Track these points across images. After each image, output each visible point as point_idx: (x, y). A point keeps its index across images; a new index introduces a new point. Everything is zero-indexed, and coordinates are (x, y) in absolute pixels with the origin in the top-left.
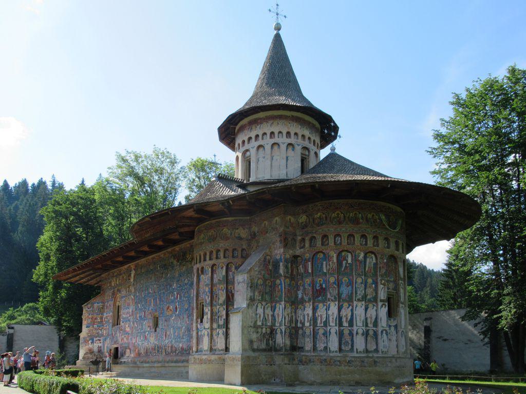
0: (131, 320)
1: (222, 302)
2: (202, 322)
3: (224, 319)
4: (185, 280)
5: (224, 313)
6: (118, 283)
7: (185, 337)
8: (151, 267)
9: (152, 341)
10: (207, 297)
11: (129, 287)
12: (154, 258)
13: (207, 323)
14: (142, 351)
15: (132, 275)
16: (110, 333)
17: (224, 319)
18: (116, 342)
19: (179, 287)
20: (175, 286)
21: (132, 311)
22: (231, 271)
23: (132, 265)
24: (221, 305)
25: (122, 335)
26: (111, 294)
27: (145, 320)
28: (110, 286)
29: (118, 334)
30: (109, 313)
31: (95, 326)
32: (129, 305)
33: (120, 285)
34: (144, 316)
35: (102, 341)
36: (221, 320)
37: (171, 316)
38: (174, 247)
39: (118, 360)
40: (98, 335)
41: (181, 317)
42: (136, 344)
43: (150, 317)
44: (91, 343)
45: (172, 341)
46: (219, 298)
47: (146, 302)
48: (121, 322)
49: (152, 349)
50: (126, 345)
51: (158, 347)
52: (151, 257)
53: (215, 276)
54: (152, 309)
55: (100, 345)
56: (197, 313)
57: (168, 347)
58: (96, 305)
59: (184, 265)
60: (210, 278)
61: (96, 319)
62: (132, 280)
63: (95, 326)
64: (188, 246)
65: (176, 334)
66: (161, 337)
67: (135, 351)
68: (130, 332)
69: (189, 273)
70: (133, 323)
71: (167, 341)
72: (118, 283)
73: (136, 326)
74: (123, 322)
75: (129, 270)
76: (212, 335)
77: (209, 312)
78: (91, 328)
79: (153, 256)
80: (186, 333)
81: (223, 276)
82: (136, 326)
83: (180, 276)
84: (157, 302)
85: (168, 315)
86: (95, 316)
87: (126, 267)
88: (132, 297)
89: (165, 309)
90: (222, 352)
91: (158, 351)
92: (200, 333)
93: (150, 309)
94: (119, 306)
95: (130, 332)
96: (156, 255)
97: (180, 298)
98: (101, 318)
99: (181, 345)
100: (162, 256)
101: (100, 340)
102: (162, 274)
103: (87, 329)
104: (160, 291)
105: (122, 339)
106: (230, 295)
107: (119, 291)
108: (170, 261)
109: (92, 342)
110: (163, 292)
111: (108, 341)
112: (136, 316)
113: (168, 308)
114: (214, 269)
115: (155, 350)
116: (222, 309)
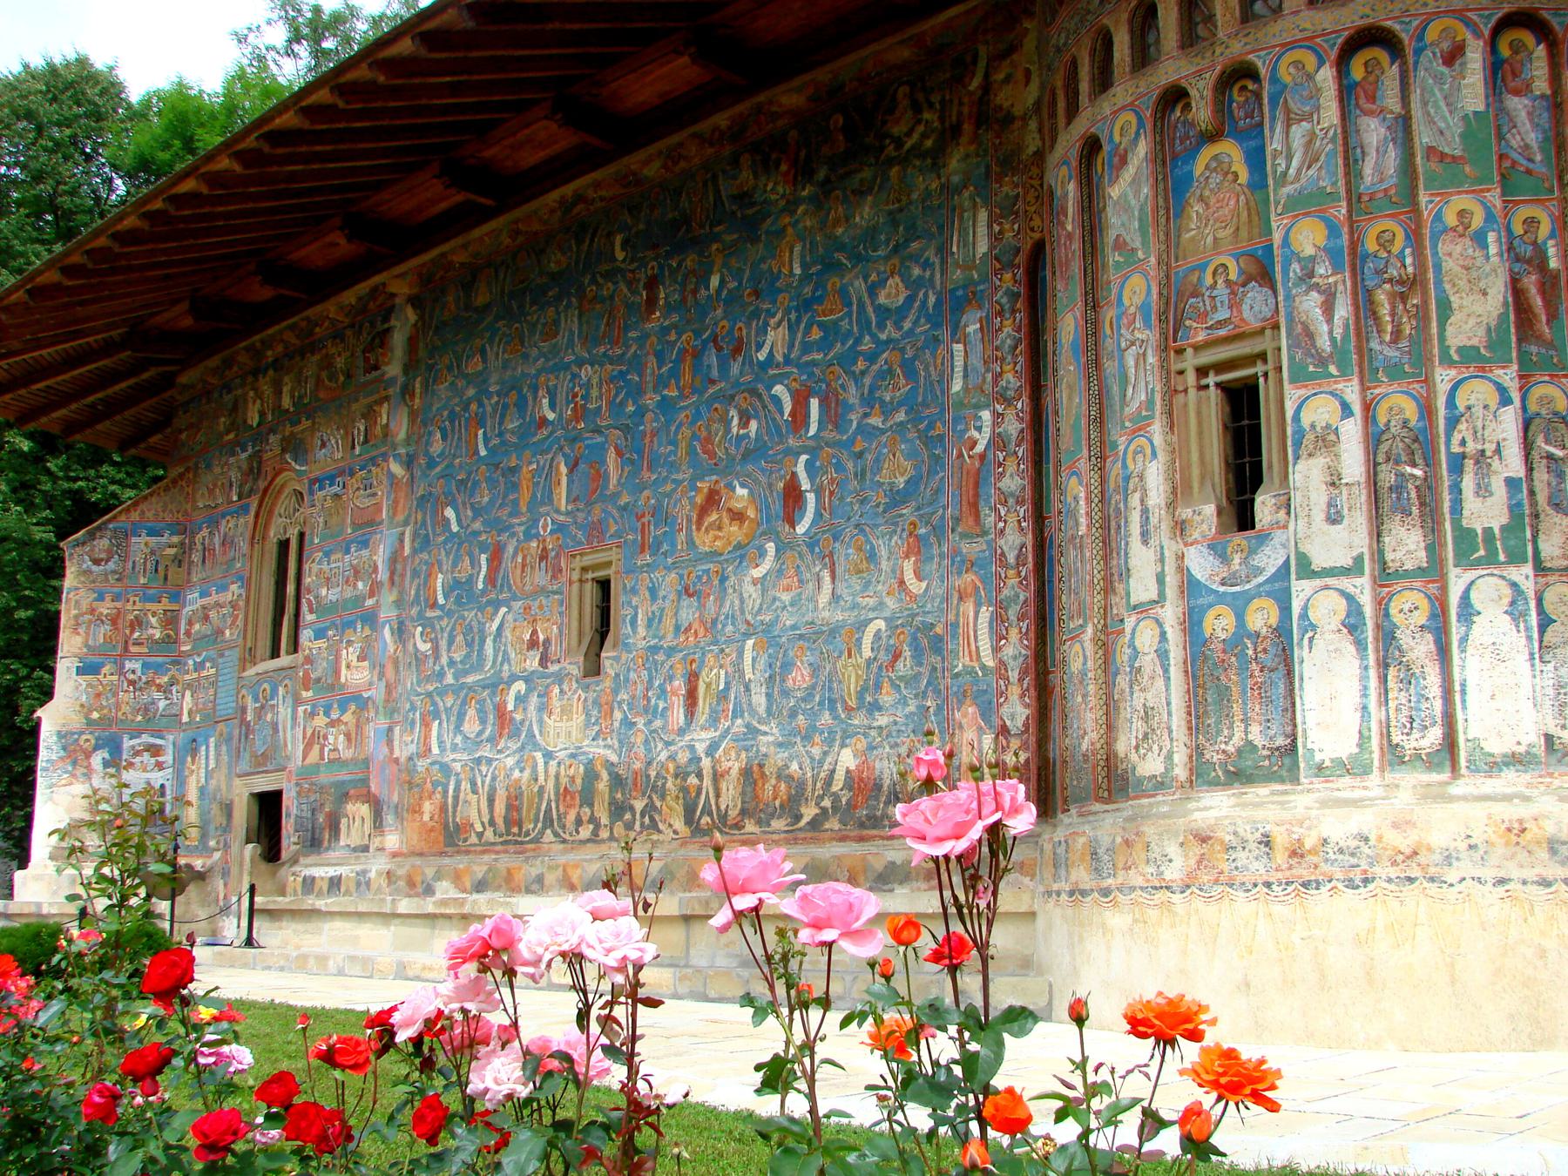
0: (387, 612)
1: (1477, 338)
2: (1243, 518)
3: (1511, 483)
4: (873, 291)
5: (1508, 425)
6: (286, 402)
7: (887, 698)
8: (555, 261)
9: (569, 732)
10: (1311, 304)
11: (370, 414)
12: (579, 198)
13: (1334, 519)
14: (473, 811)
15: (398, 340)
16: (227, 705)
17: (1511, 483)
18: (262, 762)
19: (824, 345)
20: (776, 339)
21: (394, 559)
22: (1524, 90)
23: (398, 282)
24: (1473, 361)
25: (312, 715)
26: (234, 475)
27: (497, 605)
28: (233, 427)
29: (284, 712)
30: (224, 588)
31: (128, 665)
32: (367, 524)
33: (306, 410)
34: (491, 580)
35: (168, 758)
36: (1483, 490)
37: (744, 553)
38: (762, 98)
39: (284, 872)
40: (151, 722)
41: (846, 554)
42: (421, 764)
43: (541, 577)
44: (106, 764)
45: (752, 732)
46: (1445, 309)
47: (515, 487)
48: (306, 635)
49: (564, 794)
50: (343, 776)
51: (617, 781)
52: (554, 195)
53: (1373, 131)
54: (560, 528)
55: (158, 778)
56: (1177, 453)
57: (717, 777)
58: (140, 544)
59: (860, 193)
60: (1328, 148)
61: (138, 623)
62: (393, 369)
63: (128, 665)
64: (906, 53)
65: (800, 677)
66: (650, 711)
67: (416, 810)
68: (377, 693)
69: (913, 234)
70: (401, 632)
71: (701, 738)
72: (286, 402)
73: (424, 647)
74: (320, 634)
75: (379, 312)
76: (1387, 635)
77: (1351, 431)
78: (108, 673)
79: (568, 190)
80: (904, 667)
81: (1472, 123)
82: (424, 647)
83: (831, 267)
84: (600, 477)
85: (714, 555)
86: (133, 608)
87: (350, 297)
88: (396, 469)
89: (684, 509)
90: (1511, 780)
91: (618, 810)
92: (1219, 624)
93: (545, 526)
94: (284, 545)
95: (377, 693)
96: (597, 175)
97: (834, 414)
98: (170, 620)
99: (847, 760)
100: (652, 171)
101: (155, 751)
102: (652, 284)
103: (81, 679)
104: (639, 391)
105: (313, 739)
106: (1530, 283)
107: (296, 447)
108: (727, 188)
109: (114, 762)
110: (666, 405)
111: (209, 754)
112: (428, 583)
113: (712, 499)
114: (1357, 71)
115: (588, 798)
116: (1477, 393)
